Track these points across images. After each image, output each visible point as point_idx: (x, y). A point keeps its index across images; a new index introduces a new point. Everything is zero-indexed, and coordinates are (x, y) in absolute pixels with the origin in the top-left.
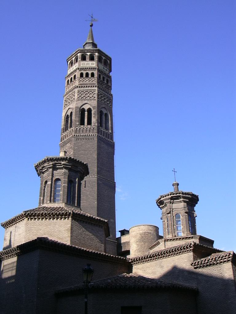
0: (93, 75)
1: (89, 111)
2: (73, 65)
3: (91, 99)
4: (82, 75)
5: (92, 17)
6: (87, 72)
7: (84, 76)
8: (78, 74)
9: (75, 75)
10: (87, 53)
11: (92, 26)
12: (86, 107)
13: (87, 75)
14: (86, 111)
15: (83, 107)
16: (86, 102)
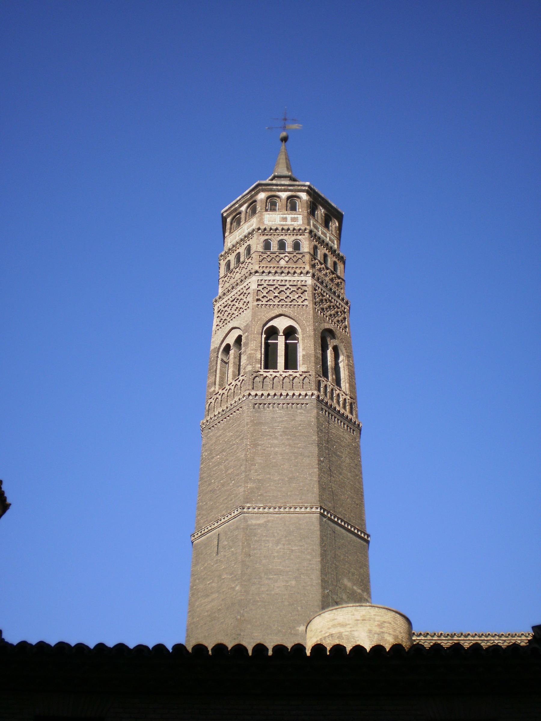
0: (297, 246)
1: (290, 332)
2: (241, 224)
3: (294, 303)
4: (267, 245)
5: (285, 119)
6: (281, 238)
7: (274, 247)
8: (257, 244)
9: (249, 246)
12: (281, 324)
13: (282, 245)
14: (281, 334)
16: (281, 312)
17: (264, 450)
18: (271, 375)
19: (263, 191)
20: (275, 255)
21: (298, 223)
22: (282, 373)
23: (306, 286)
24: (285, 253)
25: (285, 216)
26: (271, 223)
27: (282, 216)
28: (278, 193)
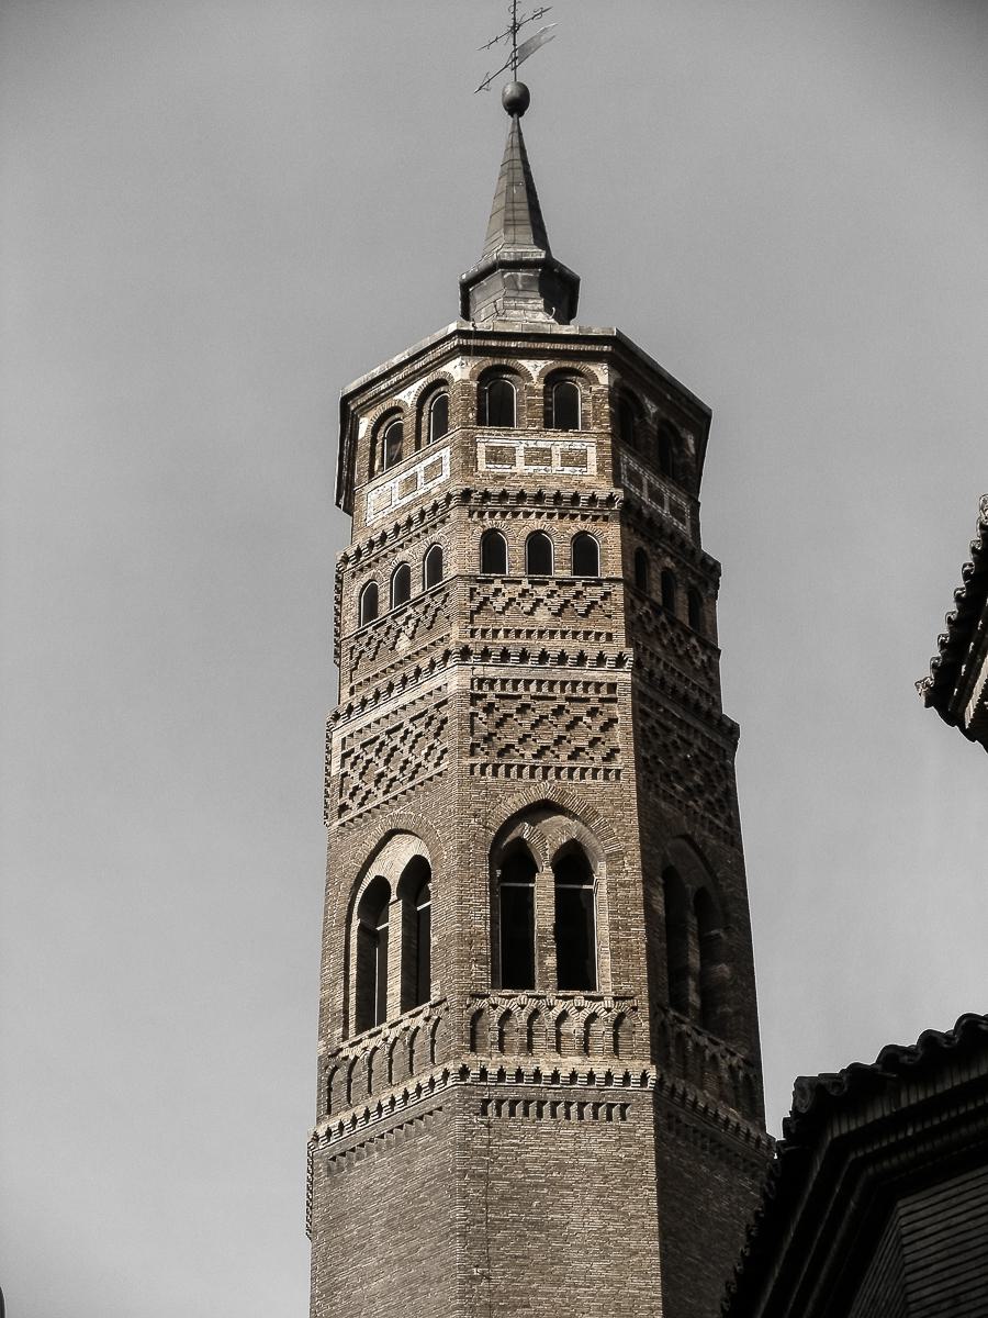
0: (435, 560)
5: (515, 29)
10: (402, 396)
11: (517, 105)
12: (392, 865)
15: (525, 831)
17: (348, 1297)
18: (365, 1049)
19: (364, 409)
20: (384, 628)
21: (440, 480)
22: (387, 1031)
23: (445, 702)
24: (405, 611)
25: (411, 472)
26: (380, 515)
27: (404, 476)
28: (396, 397)
